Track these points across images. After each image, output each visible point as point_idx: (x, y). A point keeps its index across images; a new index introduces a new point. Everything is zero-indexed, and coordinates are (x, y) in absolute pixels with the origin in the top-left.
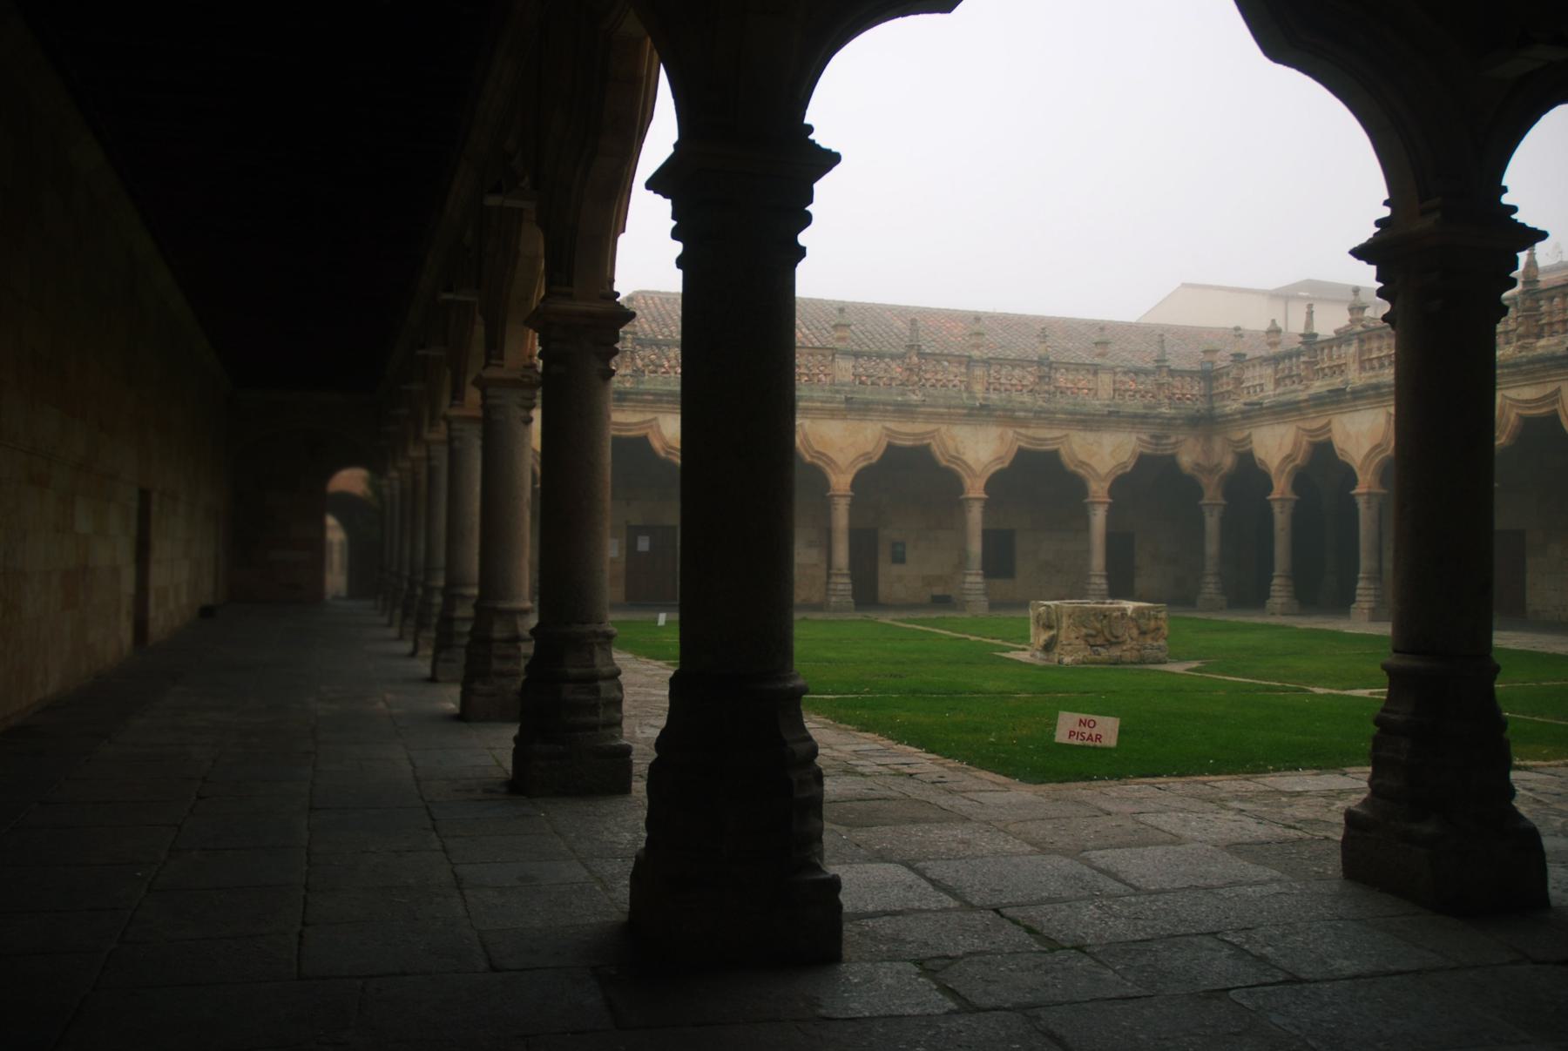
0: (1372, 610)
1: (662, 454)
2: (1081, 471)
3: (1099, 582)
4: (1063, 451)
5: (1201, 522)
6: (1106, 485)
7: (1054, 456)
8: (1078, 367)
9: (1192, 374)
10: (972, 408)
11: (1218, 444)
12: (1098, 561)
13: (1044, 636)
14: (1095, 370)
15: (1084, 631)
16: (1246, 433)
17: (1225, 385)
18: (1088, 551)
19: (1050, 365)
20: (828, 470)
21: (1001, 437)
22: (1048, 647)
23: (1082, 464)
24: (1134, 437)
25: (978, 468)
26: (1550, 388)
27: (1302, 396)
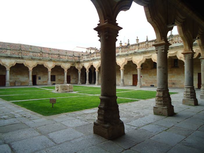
1: (2, 65)
3: (66, 81)
7: (60, 66)
8: (63, 55)
9: (77, 57)
11: (80, 65)
12: (66, 79)
13: (57, 89)
14: (65, 56)
15: (62, 88)
17: (81, 58)
18: (64, 78)
20: (29, 67)
21: (53, 64)
22: (57, 91)
23: (64, 67)
25: (50, 67)
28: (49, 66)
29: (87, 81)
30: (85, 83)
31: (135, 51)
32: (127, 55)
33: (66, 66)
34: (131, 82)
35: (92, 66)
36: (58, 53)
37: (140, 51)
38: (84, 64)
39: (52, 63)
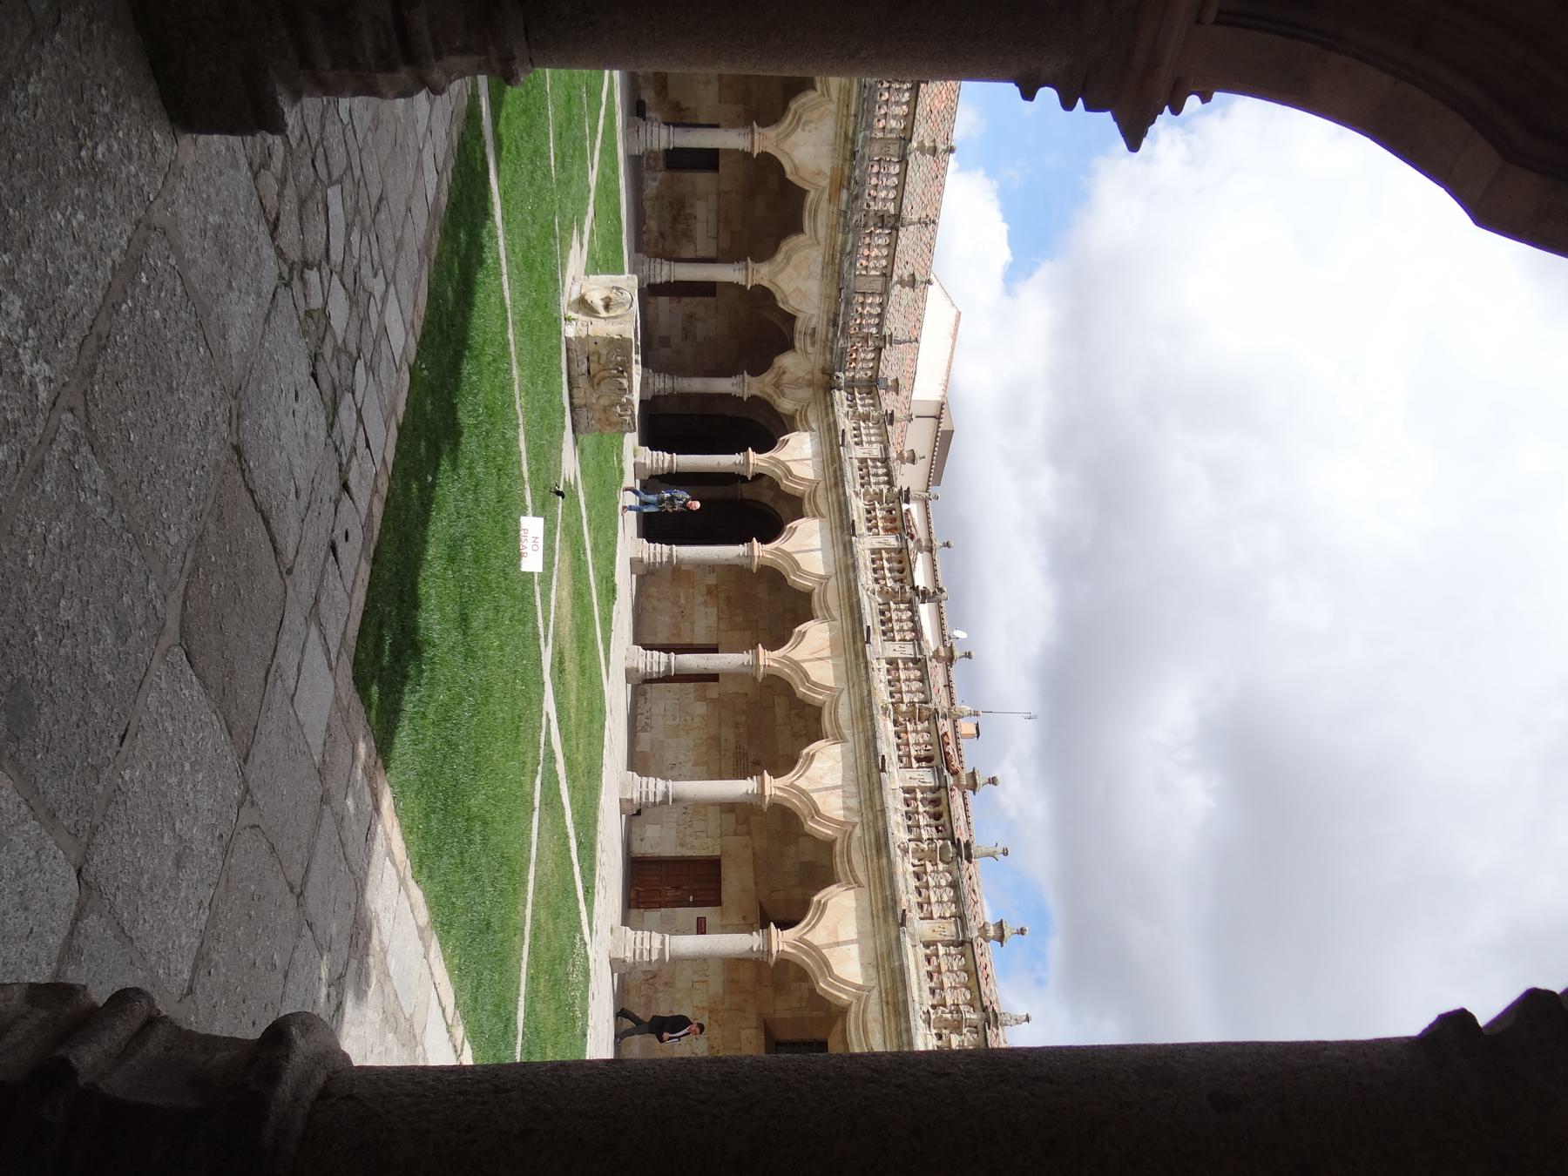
0: (641, 560)
2: (780, 257)
3: (667, 272)
4: (802, 238)
5: (728, 375)
6: (765, 284)
7: (798, 228)
8: (891, 258)
9: (876, 369)
10: (854, 142)
11: (805, 393)
13: (596, 298)
16: (814, 426)
19: (895, 228)
22: (583, 305)
23: (788, 259)
24: (814, 311)
25: (786, 146)
26: (847, 732)
27: (849, 491)
28: (800, 136)
29: (664, 460)
30: (652, 439)
31: (914, 915)
32: (881, 843)
33: (796, 278)
34: (660, 842)
35: (795, 507)
36: (912, 212)
37: (914, 959)
38: (807, 428)
39: (826, 165)
